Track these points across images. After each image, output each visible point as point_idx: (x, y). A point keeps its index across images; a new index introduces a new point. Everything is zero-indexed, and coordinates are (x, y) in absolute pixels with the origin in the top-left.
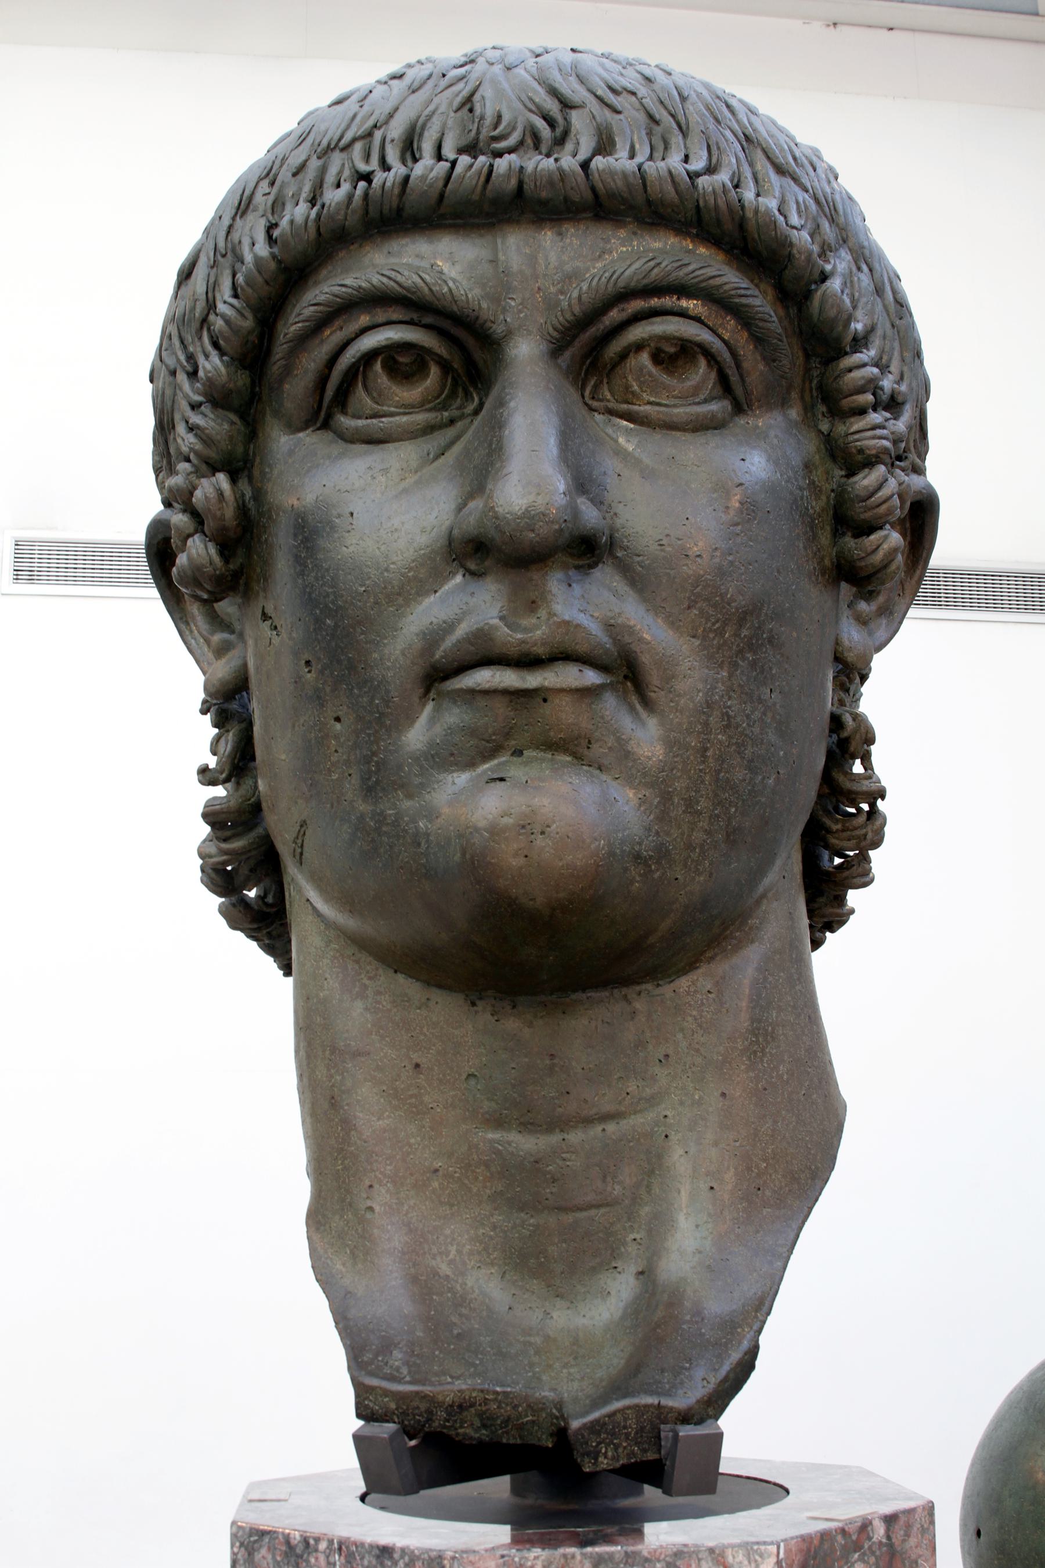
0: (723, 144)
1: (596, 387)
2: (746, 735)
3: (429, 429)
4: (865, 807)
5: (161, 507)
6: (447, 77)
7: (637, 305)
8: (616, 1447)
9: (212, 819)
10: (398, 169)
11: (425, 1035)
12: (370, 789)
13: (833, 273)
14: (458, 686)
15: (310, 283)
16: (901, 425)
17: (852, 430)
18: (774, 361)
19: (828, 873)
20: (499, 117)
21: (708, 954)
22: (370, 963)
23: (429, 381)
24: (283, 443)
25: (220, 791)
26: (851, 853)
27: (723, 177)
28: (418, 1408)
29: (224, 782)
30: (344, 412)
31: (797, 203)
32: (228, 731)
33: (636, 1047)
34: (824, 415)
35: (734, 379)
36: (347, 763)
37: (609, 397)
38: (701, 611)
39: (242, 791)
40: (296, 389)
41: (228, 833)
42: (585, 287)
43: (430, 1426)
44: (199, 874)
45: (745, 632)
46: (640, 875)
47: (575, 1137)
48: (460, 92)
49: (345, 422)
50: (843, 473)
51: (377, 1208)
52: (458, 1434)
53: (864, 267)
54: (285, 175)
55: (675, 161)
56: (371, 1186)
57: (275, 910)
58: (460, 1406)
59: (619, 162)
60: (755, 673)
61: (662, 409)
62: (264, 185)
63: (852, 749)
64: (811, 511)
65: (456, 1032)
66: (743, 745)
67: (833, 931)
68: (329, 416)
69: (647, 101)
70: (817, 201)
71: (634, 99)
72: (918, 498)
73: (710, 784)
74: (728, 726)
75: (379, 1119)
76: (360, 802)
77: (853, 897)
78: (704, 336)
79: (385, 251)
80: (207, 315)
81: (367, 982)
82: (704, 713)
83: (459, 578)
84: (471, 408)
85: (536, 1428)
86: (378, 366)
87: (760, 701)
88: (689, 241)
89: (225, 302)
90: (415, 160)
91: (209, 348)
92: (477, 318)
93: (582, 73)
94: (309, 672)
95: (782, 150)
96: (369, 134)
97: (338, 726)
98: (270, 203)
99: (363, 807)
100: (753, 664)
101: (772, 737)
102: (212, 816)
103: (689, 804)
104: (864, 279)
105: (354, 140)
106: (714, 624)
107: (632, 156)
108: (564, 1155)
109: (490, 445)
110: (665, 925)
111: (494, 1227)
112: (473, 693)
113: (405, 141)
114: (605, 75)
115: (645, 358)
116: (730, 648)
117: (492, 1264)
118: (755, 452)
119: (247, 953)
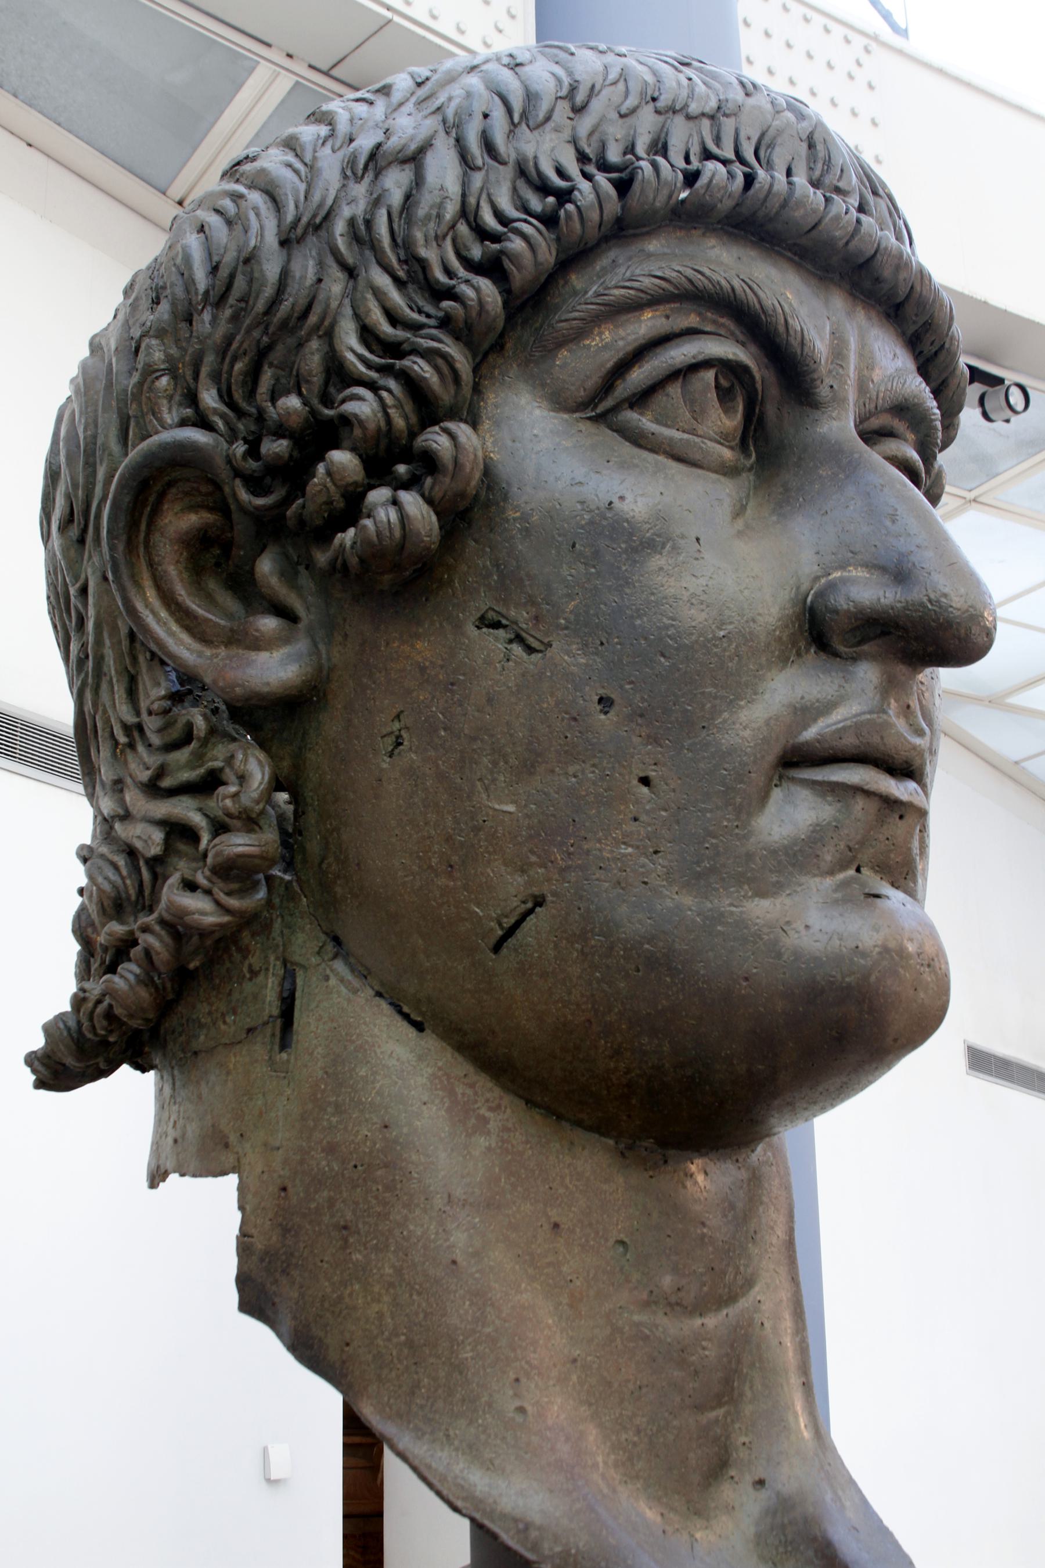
11: (567, 1188)
22: (491, 1090)
47: (711, 1321)
49: (644, 421)
56: (517, 1380)
65: (605, 1187)
81: (488, 1114)
86: (709, 375)
92: (814, 371)
108: (704, 1343)
111: (638, 1432)
117: (637, 1477)
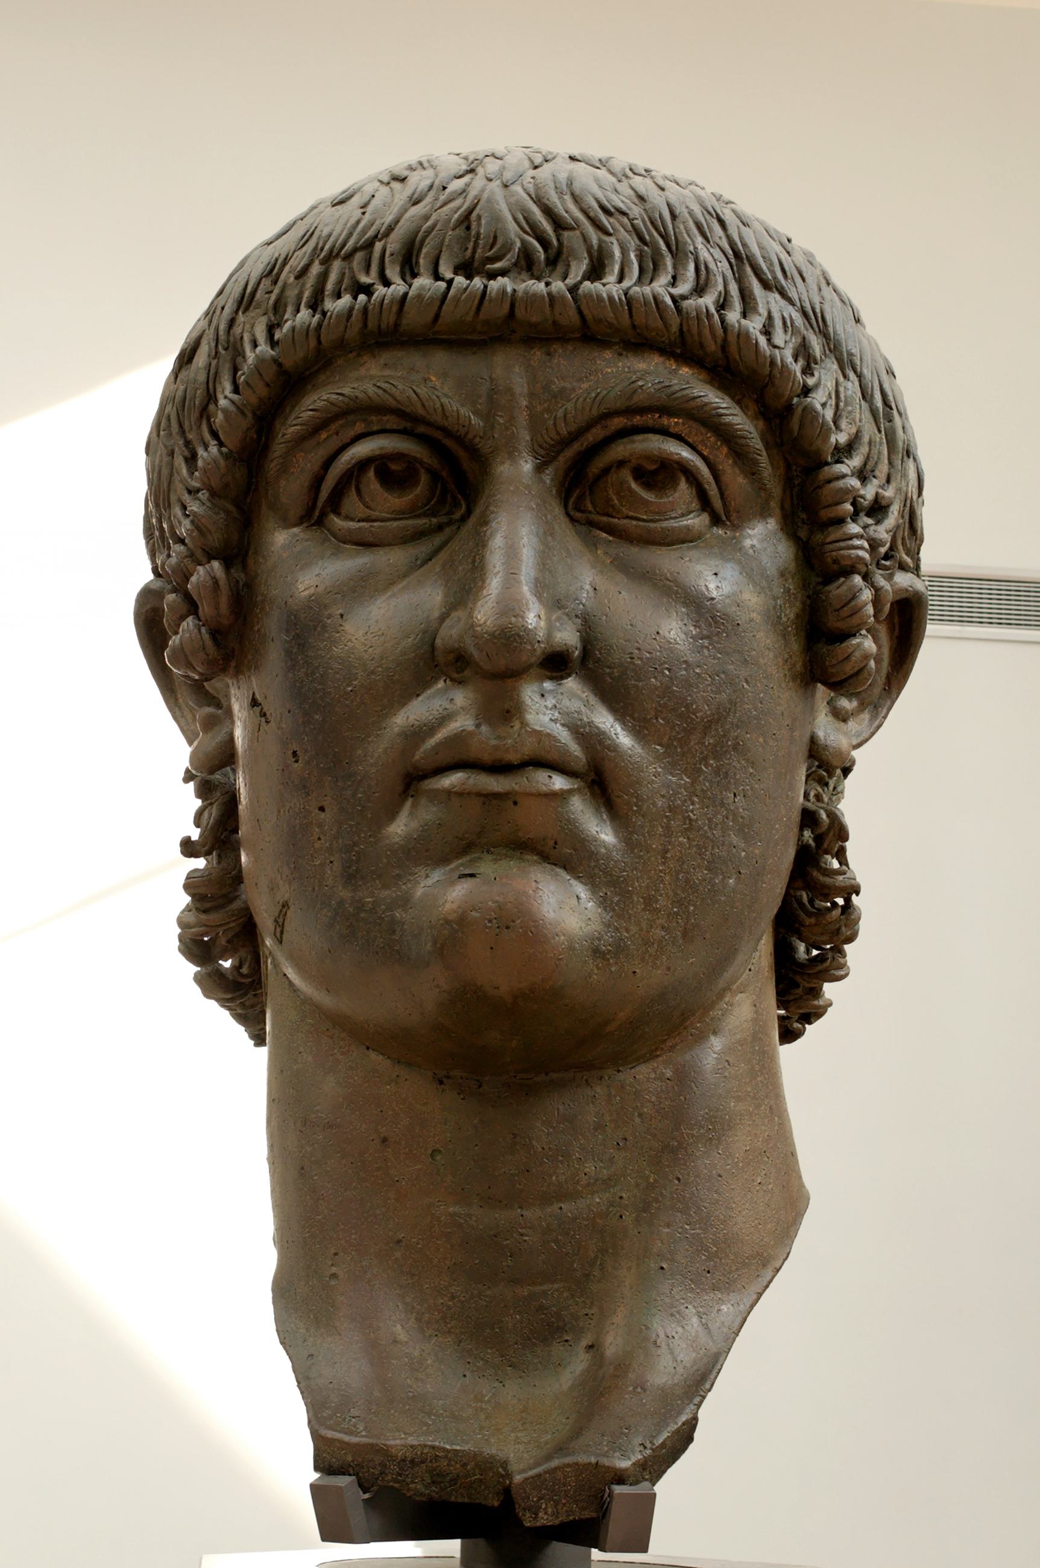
0: (712, 265)
1: (581, 498)
3: (417, 536)
4: (840, 901)
5: (151, 577)
6: (447, 191)
7: (618, 422)
8: (556, 1503)
9: (193, 891)
10: (398, 287)
11: (394, 1110)
12: (351, 876)
13: (817, 386)
14: (435, 787)
15: (309, 387)
16: (882, 532)
17: (829, 540)
18: (753, 474)
19: (801, 965)
20: (495, 237)
21: (669, 1043)
22: (343, 1039)
23: (419, 489)
24: (281, 540)
25: (200, 863)
26: (828, 946)
27: (708, 301)
28: (372, 1460)
29: (206, 854)
30: (338, 514)
31: (783, 318)
32: (211, 804)
33: (596, 1129)
34: (803, 522)
35: (713, 491)
37: (590, 508)
39: (224, 864)
40: (291, 487)
41: (208, 905)
42: (569, 406)
43: (383, 1480)
44: (178, 943)
46: (598, 969)
47: (532, 1214)
48: (459, 208)
50: (820, 580)
51: (341, 1274)
52: (409, 1490)
53: (852, 375)
54: (287, 275)
55: (660, 286)
56: (336, 1254)
58: (412, 1461)
59: (609, 287)
61: (641, 523)
62: (266, 283)
63: (825, 846)
64: (784, 619)
67: (810, 1023)
68: (323, 515)
69: (638, 222)
70: (805, 314)
71: (625, 220)
72: (904, 596)
75: (346, 1190)
76: (340, 888)
77: (829, 990)
78: (686, 454)
79: (382, 361)
80: (207, 405)
81: (340, 1057)
83: (441, 684)
84: (457, 515)
85: (483, 1487)
86: (371, 474)
87: (722, 804)
88: (672, 361)
89: (226, 397)
90: (415, 275)
91: (207, 436)
93: (577, 192)
94: (297, 761)
95: (771, 265)
96: (369, 245)
97: (323, 815)
98: (271, 302)
99: (344, 893)
100: (717, 771)
101: (734, 839)
102: (192, 884)
103: (649, 901)
104: (851, 387)
105: (355, 250)
106: (678, 733)
107: (620, 280)
109: (474, 561)
112: (449, 793)
113: (404, 256)
114: (600, 195)
115: (626, 475)
116: (694, 756)
118: (729, 565)
119: (220, 1023)
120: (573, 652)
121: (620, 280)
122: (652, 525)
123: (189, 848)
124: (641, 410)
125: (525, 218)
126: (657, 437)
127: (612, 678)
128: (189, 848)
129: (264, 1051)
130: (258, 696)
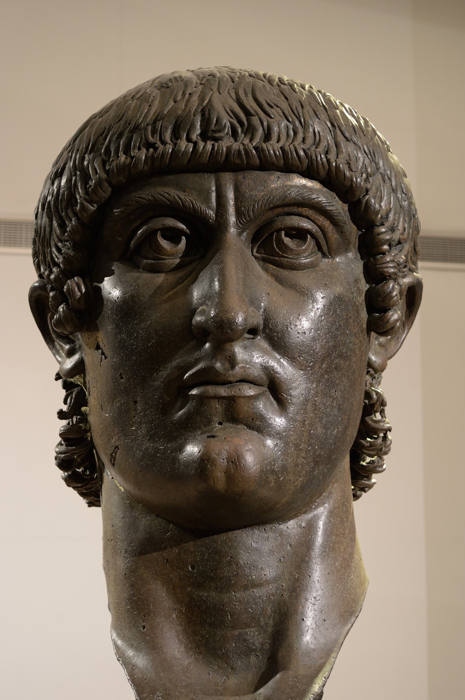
2: (324, 413)
18: (342, 233)
36: (140, 423)
38: (304, 358)
45: (324, 366)
46: (274, 479)
57: (89, 477)
60: (328, 384)
63: (375, 409)
66: (322, 417)
67: (365, 492)
73: (306, 436)
74: (315, 410)
82: (304, 404)
87: (330, 396)
90: (177, 139)
91: (71, 215)
103: (297, 446)
106: (310, 363)
107: (278, 141)
110: (284, 500)
116: (317, 374)
120: (260, 327)
121: (278, 141)
122: (294, 261)
123: (61, 415)
124: (288, 205)
125: (231, 110)
126: (297, 217)
127: (278, 338)
128: (61, 415)
129: (97, 511)
130: (101, 344)
